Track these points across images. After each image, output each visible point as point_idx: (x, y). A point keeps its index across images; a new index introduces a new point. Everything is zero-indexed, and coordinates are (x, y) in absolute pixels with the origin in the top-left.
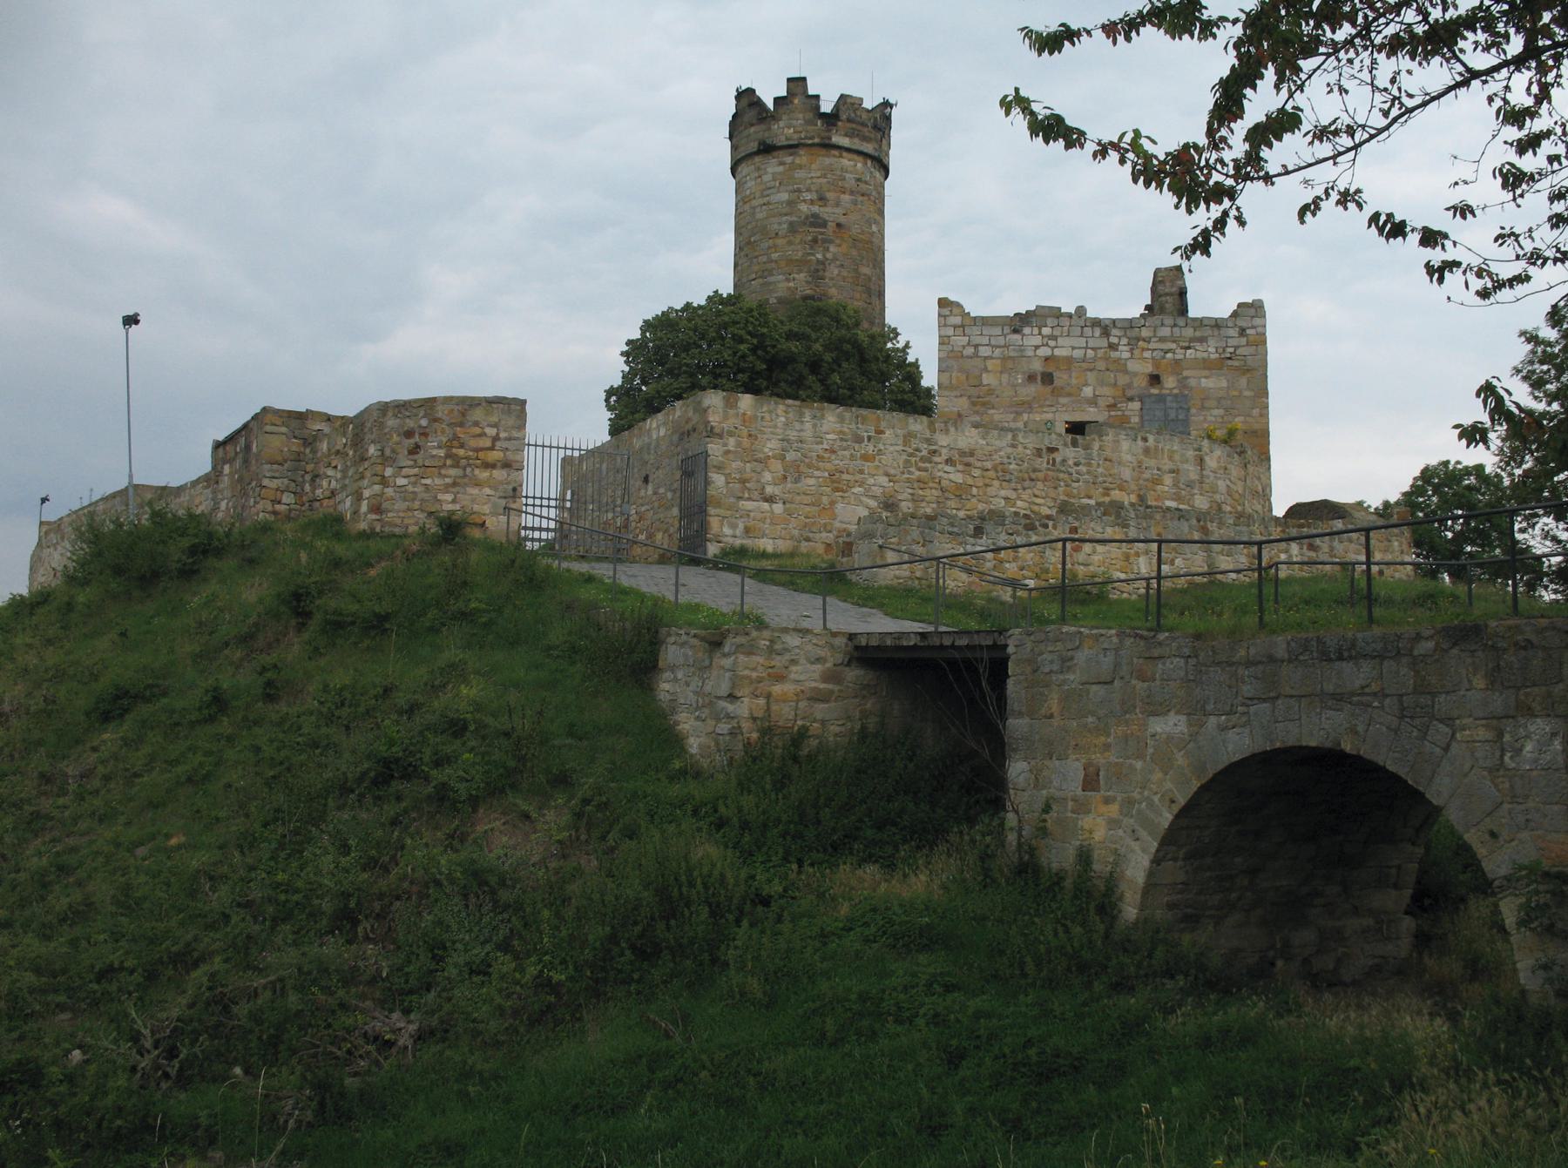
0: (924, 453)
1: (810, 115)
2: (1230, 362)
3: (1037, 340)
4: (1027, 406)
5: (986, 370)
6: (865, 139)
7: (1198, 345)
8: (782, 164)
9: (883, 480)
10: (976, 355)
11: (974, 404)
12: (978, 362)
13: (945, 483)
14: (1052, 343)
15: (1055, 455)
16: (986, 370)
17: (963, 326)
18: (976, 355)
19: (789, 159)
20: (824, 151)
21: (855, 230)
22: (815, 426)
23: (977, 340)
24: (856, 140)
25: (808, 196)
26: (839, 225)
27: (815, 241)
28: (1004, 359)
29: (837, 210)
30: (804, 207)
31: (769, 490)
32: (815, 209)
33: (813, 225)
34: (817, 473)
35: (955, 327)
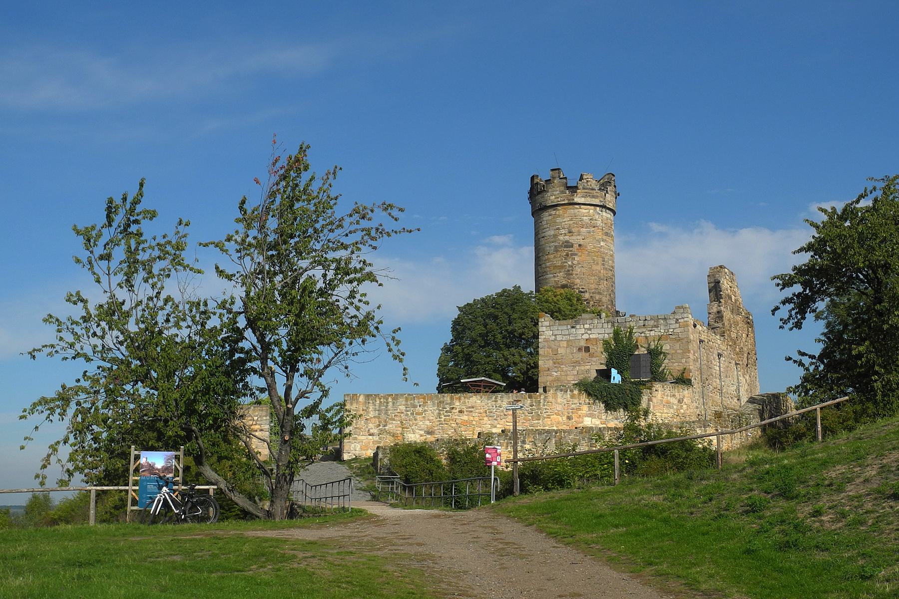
1: (562, 188)
3: (583, 331)
4: (577, 363)
6: (593, 197)
8: (550, 215)
9: (427, 423)
10: (555, 339)
11: (554, 363)
18: (555, 339)
19: (553, 212)
21: (590, 247)
23: (556, 332)
24: (588, 199)
25: (563, 231)
26: (580, 245)
27: (567, 255)
28: (568, 341)
29: (579, 237)
30: (561, 238)
31: (372, 431)
32: (567, 238)
33: (566, 247)
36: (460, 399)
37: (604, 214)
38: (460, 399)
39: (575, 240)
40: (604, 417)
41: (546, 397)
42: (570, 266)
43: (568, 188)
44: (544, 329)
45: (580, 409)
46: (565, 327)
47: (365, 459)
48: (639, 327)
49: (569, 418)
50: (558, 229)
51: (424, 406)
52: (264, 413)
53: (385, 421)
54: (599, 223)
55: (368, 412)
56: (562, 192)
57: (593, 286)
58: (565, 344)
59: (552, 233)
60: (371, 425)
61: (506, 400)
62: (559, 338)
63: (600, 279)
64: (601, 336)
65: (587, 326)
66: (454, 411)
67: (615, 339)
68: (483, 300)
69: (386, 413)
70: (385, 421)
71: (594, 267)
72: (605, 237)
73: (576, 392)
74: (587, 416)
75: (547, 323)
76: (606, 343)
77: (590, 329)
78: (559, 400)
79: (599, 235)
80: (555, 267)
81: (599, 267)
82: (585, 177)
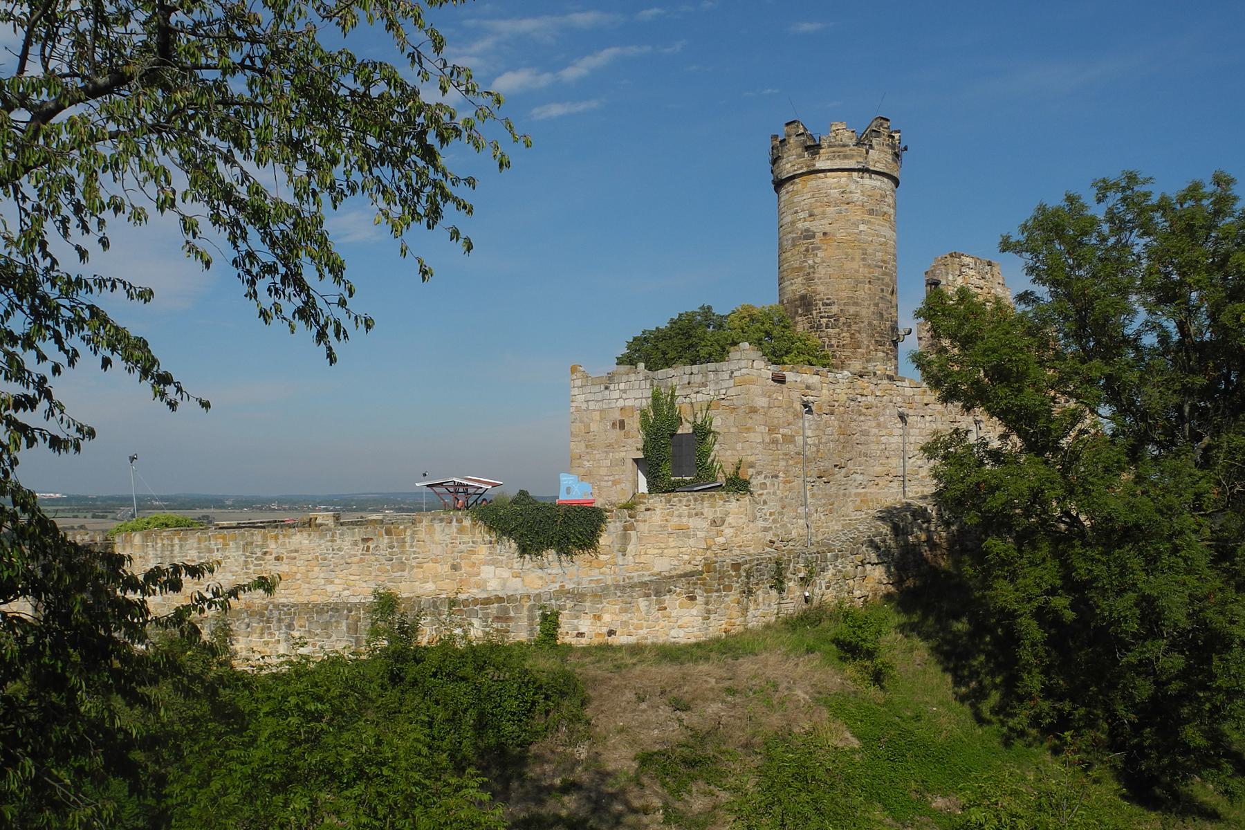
0: (259, 554)
3: (616, 394)
6: (846, 157)
9: (229, 576)
14: (624, 396)
15: (369, 544)
19: (790, 188)
22: (181, 546)
26: (825, 234)
27: (807, 250)
29: (823, 222)
30: (800, 225)
32: (807, 224)
33: (806, 238)
38: (276, 538)
39: (817, 226)
40: (516, 566)
41: (414, 533)
42: (810, 267)
43: (807, 148)
45: (473, 552)
48: (683, 388)
49: (455, 567)
50: (796, 212)
51: (224, 549)
54: (857, 196)
55: (147, 561)
57: (844, 294)
58: (596, 416)
61: (348, 539)
63: (857, 282)
64: (637, 403)
65: (622, 386)
66: (267, 557)
73: (467, 523)
74: (487, 563)
76: (644, 414)
77: (625, 391)
78: (438, 537)
79: (856, 214)
81: (855, 265)
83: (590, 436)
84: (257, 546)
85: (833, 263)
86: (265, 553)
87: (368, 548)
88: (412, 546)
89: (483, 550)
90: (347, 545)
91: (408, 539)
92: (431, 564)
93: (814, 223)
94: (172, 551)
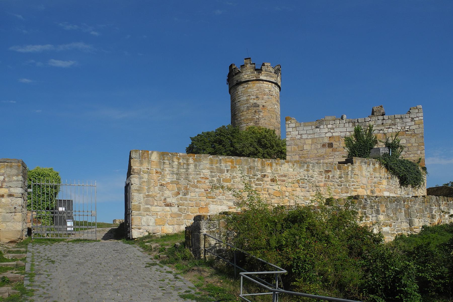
0: (259, 176)
1: (252, 70)
2: (407, 132)
3: (326, 130)
5: (305, 143)
6: (271, 77)
7: (393, 127)
10: (301, 138)
12: (302, 141)
13: (271, 191)
14: (332, 131)
16: (305, 143)
17: (296, 127)
18: (301, 138)
19: (246, 86)
20: (258, 82)
21: (269, 107)
22: (196, 166)
23: (301, 132)
24: (268, 77)
25: (252, 97)
26: (263, 106)
27: (255, 112)
29: (262, 101)
30: (251, 101)
31: (169, 201)
32: (255, 101)
33: (254, 107)
34: (197, 190)
35: (292, 128)
36: (271, 165)
37: (276, 89)
38: (271, 165)
39: (259, 102)
41: (353, 169)
43: (256, 70)
44: (290, 130)
46: (310, 128)
47: (163, 237)
48: (378, 126)
50: (249, 96)
51: (232, 171)
52: (14, 171)
53: (186, 188)
54: (274, 93)
55: (163, 176)
56: (252, 73)
58: (310, 141)
59: (245, 98)
60: (167, 193)
62: (304, 137)
64: (343, 134)
65: (330, 126)
66: (265, 179)
67: (356, 136)
68: (208, 133)
69: (186, 178)
70: (186, 188)
71: (272, 120)
72: (277, 103)
73: (377, 165)
75: (293, 125)
76: (348, 140)
78: (365, 173)
80: (247, 119)
82: (266, 64)
83: (305, 152)
84: (258, 170)
85: (266, 118)
86: (265, 176)
87: (329, 176)
88: (351, 177)
89: (385, 182)
90: (316, 174)
91: (349, 173)
92: (361, 189)
93: (259, 101)
94: (187, 169)
